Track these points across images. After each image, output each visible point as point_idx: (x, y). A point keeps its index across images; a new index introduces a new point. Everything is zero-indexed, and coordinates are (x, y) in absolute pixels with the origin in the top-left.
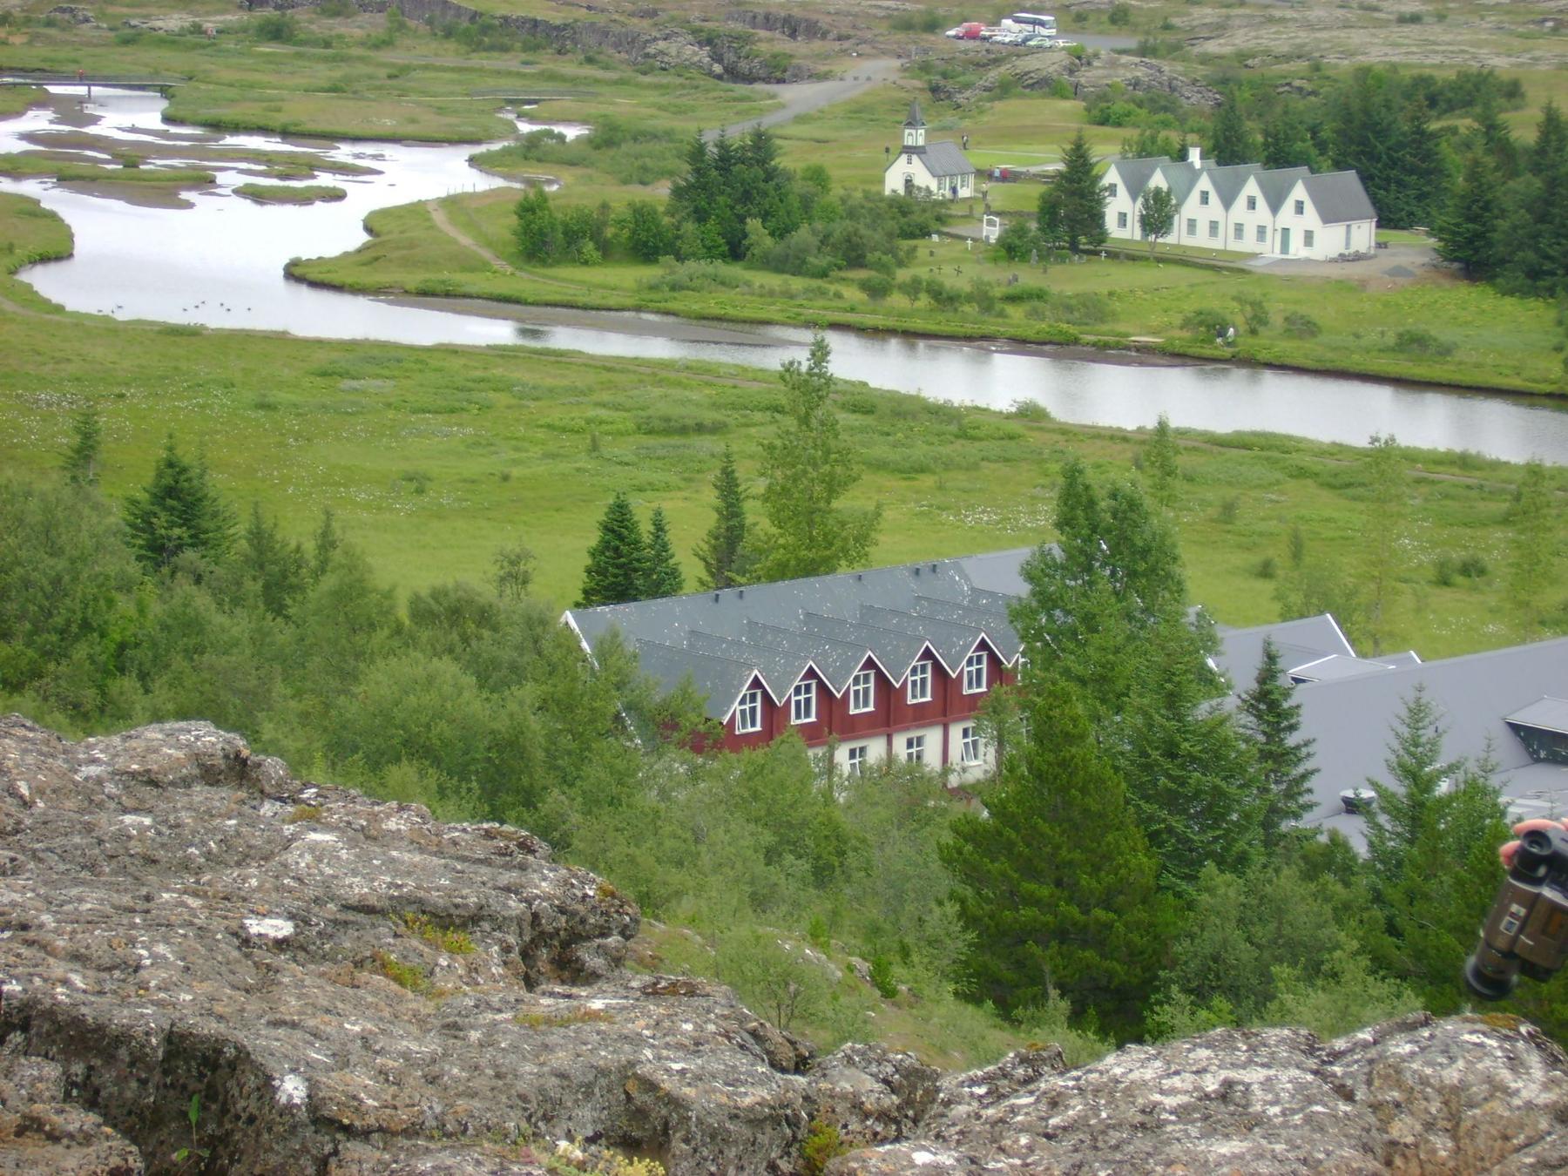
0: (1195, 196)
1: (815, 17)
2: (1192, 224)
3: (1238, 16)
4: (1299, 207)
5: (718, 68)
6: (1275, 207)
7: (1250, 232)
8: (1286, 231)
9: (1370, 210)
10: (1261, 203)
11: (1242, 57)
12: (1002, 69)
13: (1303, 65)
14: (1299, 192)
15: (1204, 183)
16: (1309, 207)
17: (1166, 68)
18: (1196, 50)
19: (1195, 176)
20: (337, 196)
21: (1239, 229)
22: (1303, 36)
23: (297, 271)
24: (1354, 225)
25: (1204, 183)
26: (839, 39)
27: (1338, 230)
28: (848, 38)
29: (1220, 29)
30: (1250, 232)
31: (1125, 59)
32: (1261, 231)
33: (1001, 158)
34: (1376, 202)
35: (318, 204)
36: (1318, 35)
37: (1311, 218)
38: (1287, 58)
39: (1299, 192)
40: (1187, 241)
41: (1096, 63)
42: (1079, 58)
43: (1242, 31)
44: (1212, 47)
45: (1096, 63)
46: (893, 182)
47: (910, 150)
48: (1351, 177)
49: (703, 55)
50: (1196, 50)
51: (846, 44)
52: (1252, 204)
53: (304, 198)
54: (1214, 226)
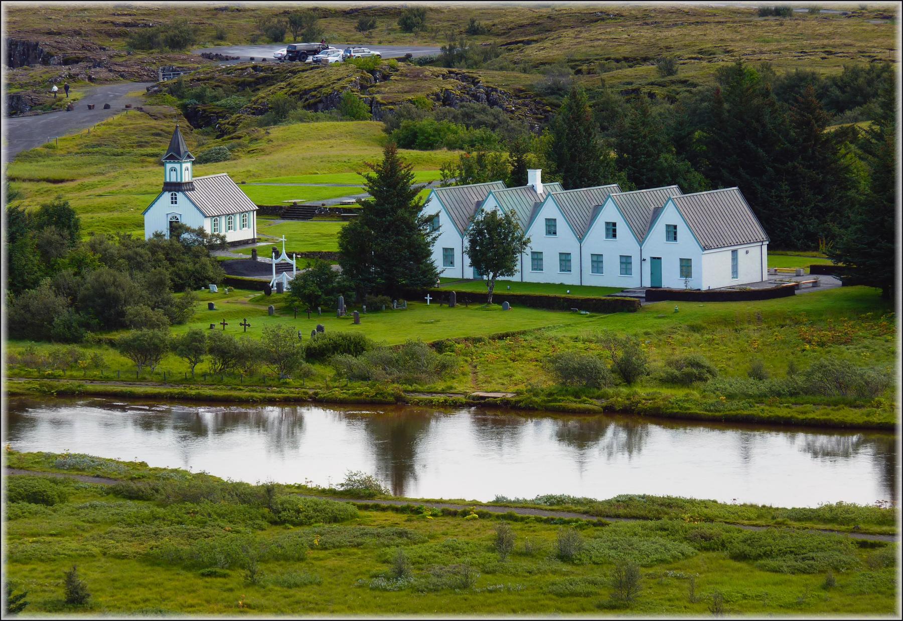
0: (539, 225)
1: (33, 39)
2: (537, 259)
6: (641, 236)
7: (611, 265)
8: (656, 261)
9: (761, 234)
13: (649, 70)
21: (597, 262)
26: (66, 62)
28: (76, 61)
30: (611, 265)
31: (429, 70)
32: (626, 262)
37: (686, 244)
40: (531, 276)
42: (372, 72)
48: (732, 197)
54: (565, 260)
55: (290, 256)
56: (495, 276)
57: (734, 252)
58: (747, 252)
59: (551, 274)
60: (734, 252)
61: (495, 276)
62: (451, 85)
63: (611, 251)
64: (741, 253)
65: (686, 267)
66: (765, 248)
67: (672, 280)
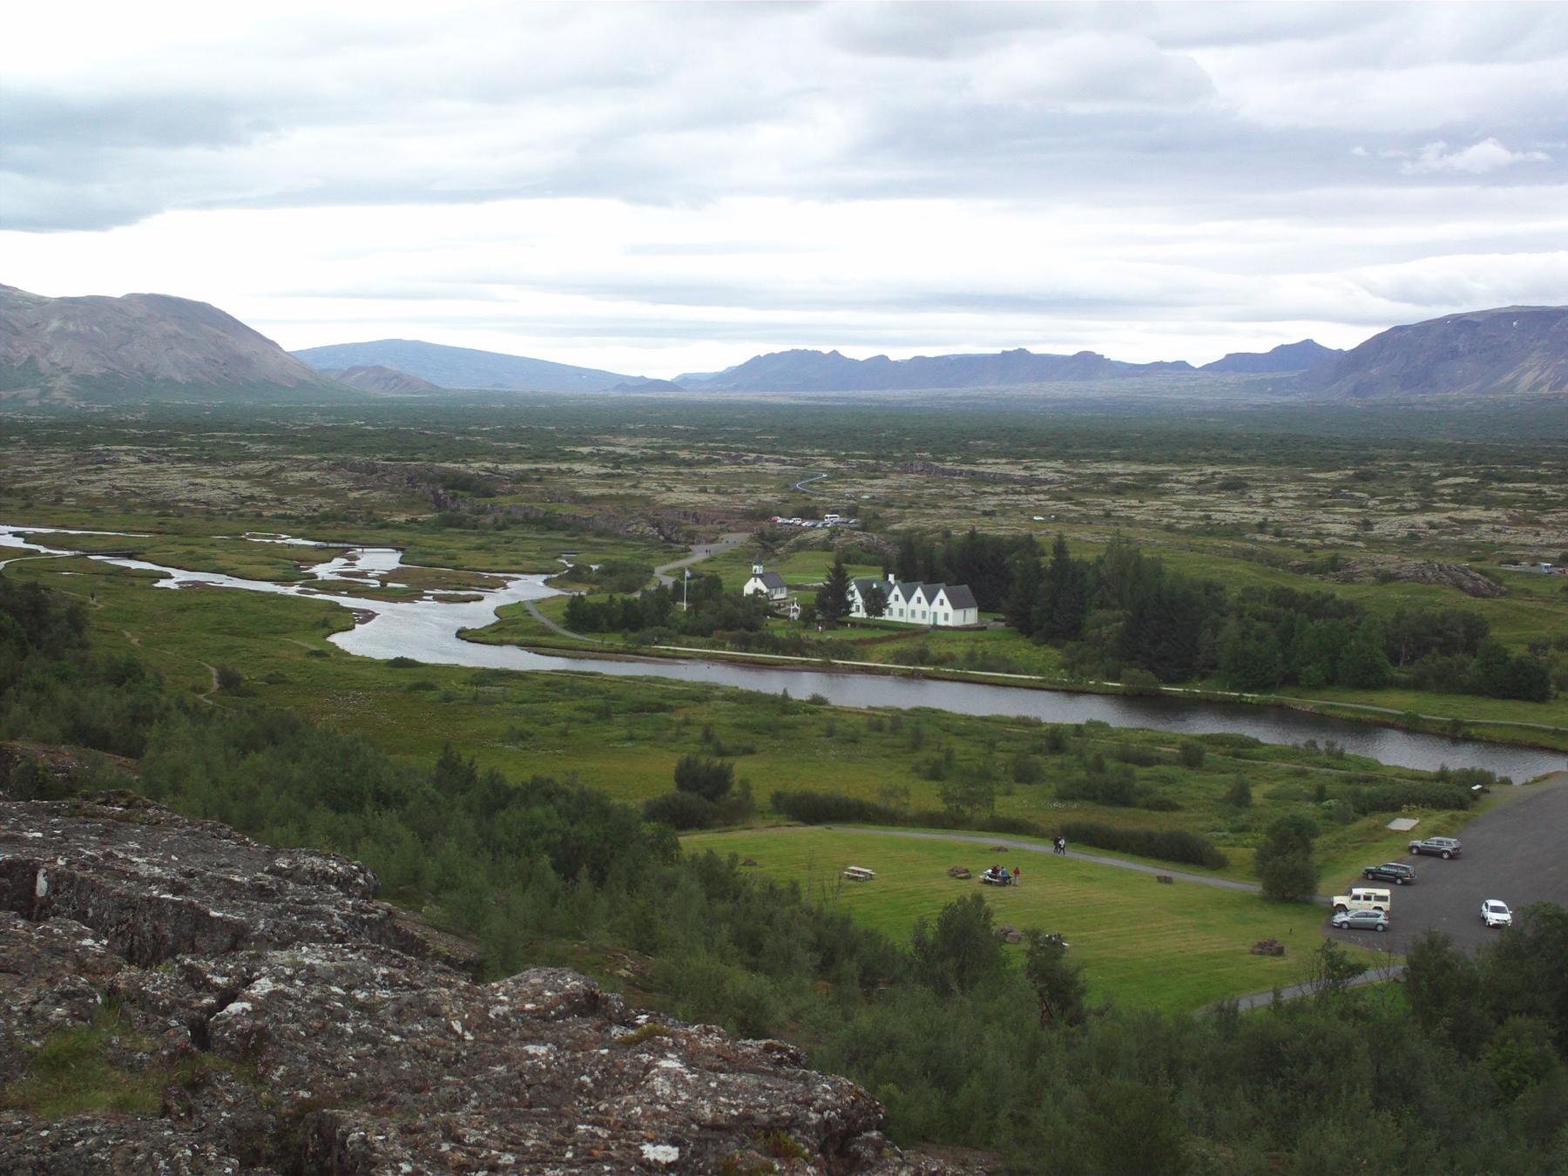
4: (942, 602)
5: (662, 538)
8: (935, 613)
10: (924, 600)
11: (911, 531)
13: (939, 534)
14: (942, 595)
15: (897, 591)
16: (946, 602)
17: (875, 537)
18: (889, 528)
19: (892, 587)
20: (480, 599)
21: (913, 613)
22: (939, 522)
23: (463, 635)
24: (968, 611)
25: (897, 591)
26: (720, 523)
27: (960, 613)
29: (900, 518)
31: (856, 533)
32: (924, 614)
33: (797, 579)
34: (978, 604)
35: (472, 603)
36: (947, 521)
37: (947, 606)
38: (933, 532)
39: (942, 595)
41: (842, 535)
44: (896, 527)
45: (842, 535)
46: (749, 588)
47: (756, 576)
49: (655, 532)
50: (889, 528)
51: (723, 526)
52: (919, 600)
53: (467, 600)
54: (901, 611)
59: (895, 617)
67: (941, 622)
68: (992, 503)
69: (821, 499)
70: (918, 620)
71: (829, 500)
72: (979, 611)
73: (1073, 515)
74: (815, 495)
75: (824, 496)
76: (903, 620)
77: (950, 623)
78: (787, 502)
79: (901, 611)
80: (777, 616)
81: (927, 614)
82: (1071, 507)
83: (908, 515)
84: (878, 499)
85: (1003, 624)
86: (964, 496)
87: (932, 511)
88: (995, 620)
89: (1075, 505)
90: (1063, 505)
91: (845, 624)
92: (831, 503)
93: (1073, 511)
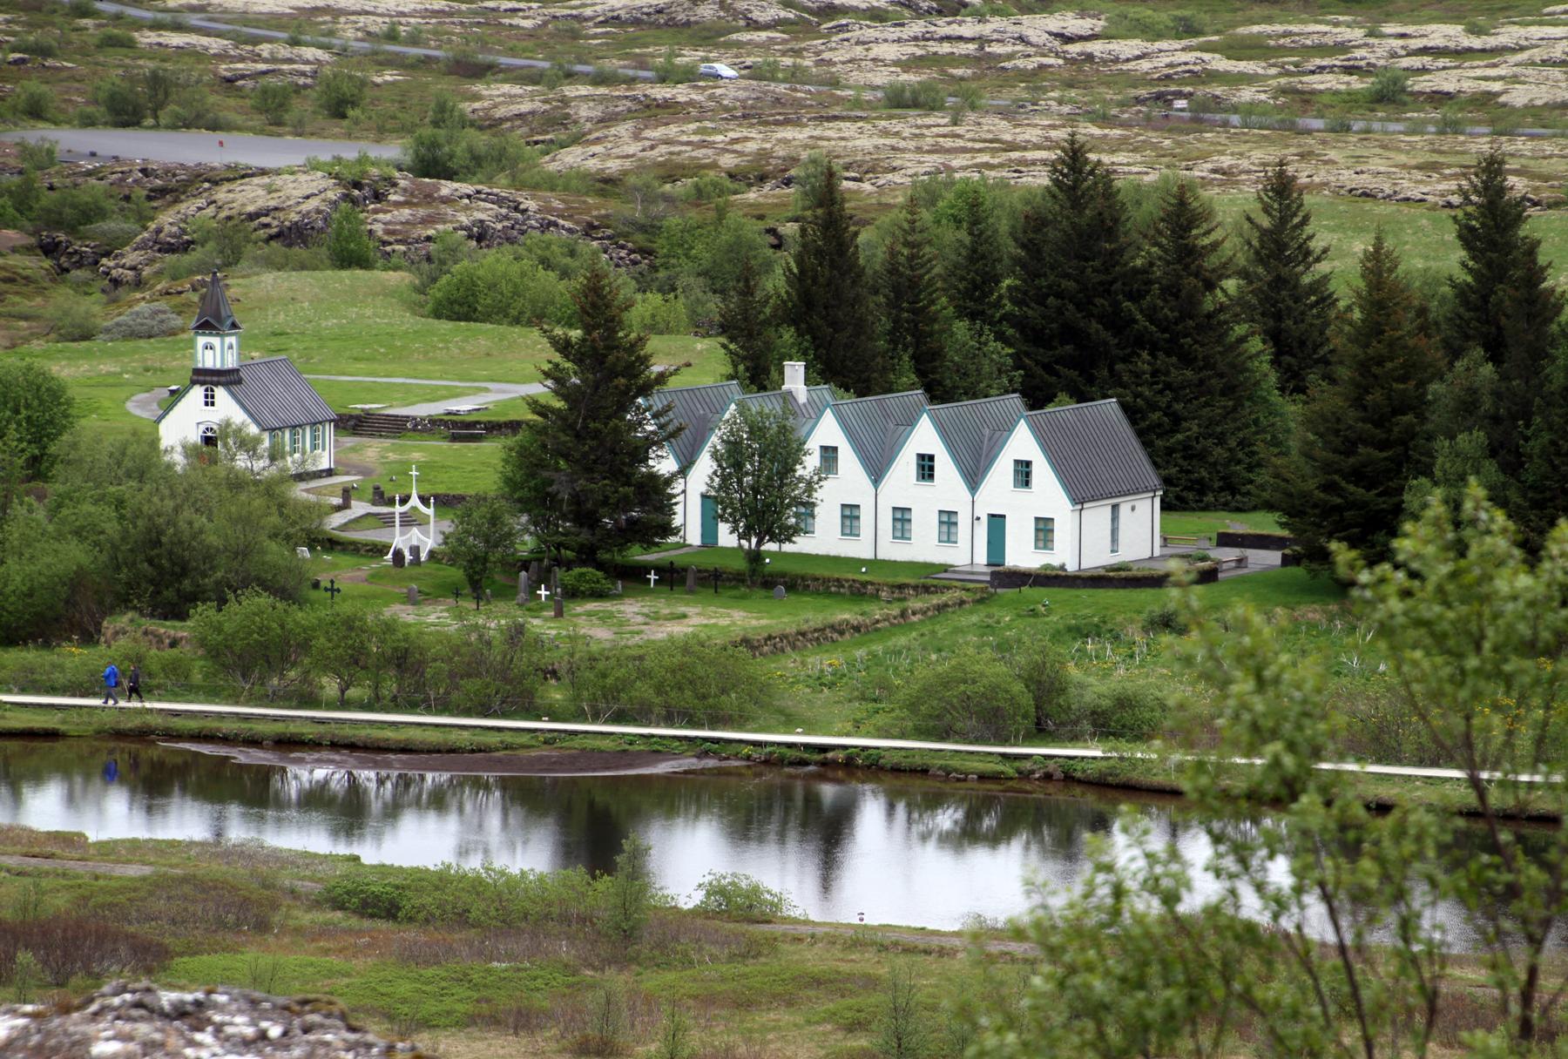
3: (585, 98)
7: (925, 526)
8: (997, 523)
12: (189, 206)
21: (902, 517)
27: (1098, 514)
30: (925, 526)
32: (948, 520)
43: (624, 129)
54: (850, 514)
55: (424, 500)
56: (759, 543)
57: (1115, 507)
58: (1133, 509)
60: (1115, 507)
61: (759, 543)
62: (485, 213)
63: (926, 502)
64: (1124, 509)
65: (1044, 530)
66: (1157, 501)
68: (890, 52)
69: (176, 39)
70: (924, 547)
71: (215, 44)
72: (1166, 507)
73: (1247, 94)
74: (139, 25)
75: (179, 28)
76: (859, 549)
77: (1063, 555)
78: (46, 52)
79: (850, 514)
80: (332, 544)
81: (963, 521)
82: (1219, 63)
83: (584, 111)
84: (414, 40)
85: (1273, 557)
86: (754, 25)
87: (681, 93)
88: (1226, 540)
89: (1236, 50)
90: (1173, 54)
91: (633, 576)
92: (222, 57)
93: (1249, 79)
